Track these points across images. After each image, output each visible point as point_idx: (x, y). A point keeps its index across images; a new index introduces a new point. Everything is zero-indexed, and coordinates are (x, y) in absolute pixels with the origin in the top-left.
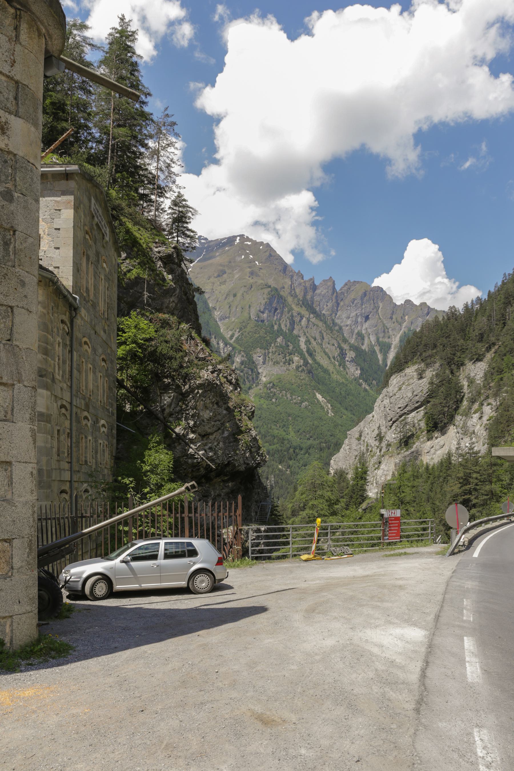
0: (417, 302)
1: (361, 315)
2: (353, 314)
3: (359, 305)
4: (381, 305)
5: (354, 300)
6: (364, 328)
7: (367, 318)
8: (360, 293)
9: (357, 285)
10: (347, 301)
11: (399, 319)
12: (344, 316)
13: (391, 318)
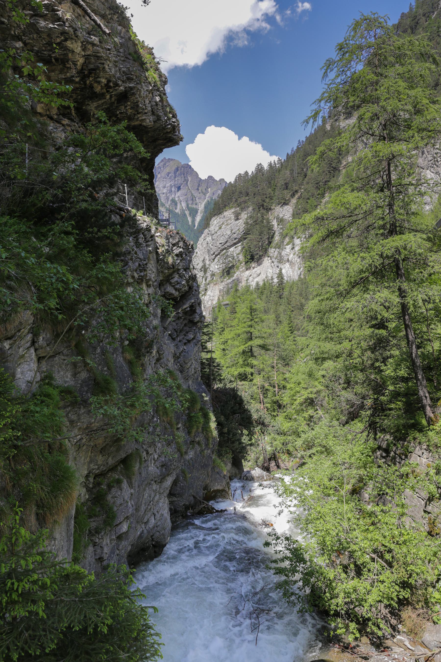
0: (217, 179)
1: (174, 185)
2: (168, 185)
3: (173, 178)
4: (190, 179)
5: (169, 173)
6: (177, 196)
7: (179, 188)
8: (174, 169)
9: (171, 162)
10: (163, 174)
11: (204, 191)
12: (161, 186)
13: (198, 189)
